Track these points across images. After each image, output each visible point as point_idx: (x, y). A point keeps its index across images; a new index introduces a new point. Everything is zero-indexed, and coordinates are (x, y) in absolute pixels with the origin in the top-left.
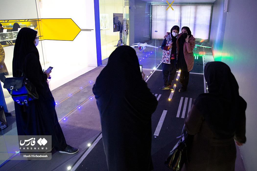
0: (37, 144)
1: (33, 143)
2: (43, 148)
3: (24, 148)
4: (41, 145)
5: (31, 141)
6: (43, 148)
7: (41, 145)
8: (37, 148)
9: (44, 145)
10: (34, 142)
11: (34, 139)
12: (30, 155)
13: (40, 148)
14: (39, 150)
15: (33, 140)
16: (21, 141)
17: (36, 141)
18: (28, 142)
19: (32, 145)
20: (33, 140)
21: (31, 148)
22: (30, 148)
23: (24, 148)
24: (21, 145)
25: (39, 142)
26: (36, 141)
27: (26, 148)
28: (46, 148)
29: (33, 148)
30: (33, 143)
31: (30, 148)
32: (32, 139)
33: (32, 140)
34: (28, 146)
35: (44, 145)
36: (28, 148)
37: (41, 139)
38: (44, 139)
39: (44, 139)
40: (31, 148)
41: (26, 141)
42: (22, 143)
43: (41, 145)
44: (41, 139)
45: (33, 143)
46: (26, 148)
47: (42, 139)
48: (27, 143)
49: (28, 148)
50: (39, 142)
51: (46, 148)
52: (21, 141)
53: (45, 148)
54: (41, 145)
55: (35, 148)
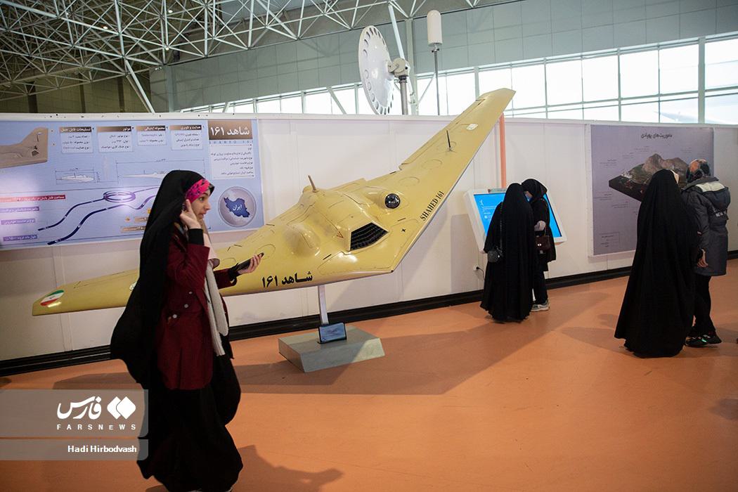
0: (106, 416)
1: (94, 413)
2: (122, 427)
3: (69, 427)
4: (117, 416)
5: (88, 405)
6: (122, 427)
7: (117, 416)
8: (106, 427)
9: (126, 416)
10: (98, 408)
11: (99, 399)
12: (86, 447)
13: (116, 427)
14: (109, 429)
15: (95, 402)
16: (60, 404)
17: (104, 405)
18: (83, 408)
19: (92, 417)
20: (95, 402)
21: (90, 427)
22: (85, 427)
23: (69, 427)
24: (61, 416)
25: (111, 408)
26: (104, 405)
27: (74, 427)
28: (133, 427)
29: (95, 427)
30: (95, 410)
31: (85, 427)
32: (92, 399)
33: (91, 402)
34: (79, 421)
35: (126, 416)
36: (80, 427)
37: (117, 400)
38: (126, 399)
39: (126, 399)
40: (90, 427)
41: (74, 405)
42: (63, 411)
43: (117, 418)
44: (117, 400)
45: (94, 413)
46: (74, 427)
47: (121, 399)
48: (77, 411)
49: (80, 427)
50: (111, 408)
51: (133, 427)
52: (60, 404)
53: (128, 427)
54: (117, 418)
55: (101, 427)
